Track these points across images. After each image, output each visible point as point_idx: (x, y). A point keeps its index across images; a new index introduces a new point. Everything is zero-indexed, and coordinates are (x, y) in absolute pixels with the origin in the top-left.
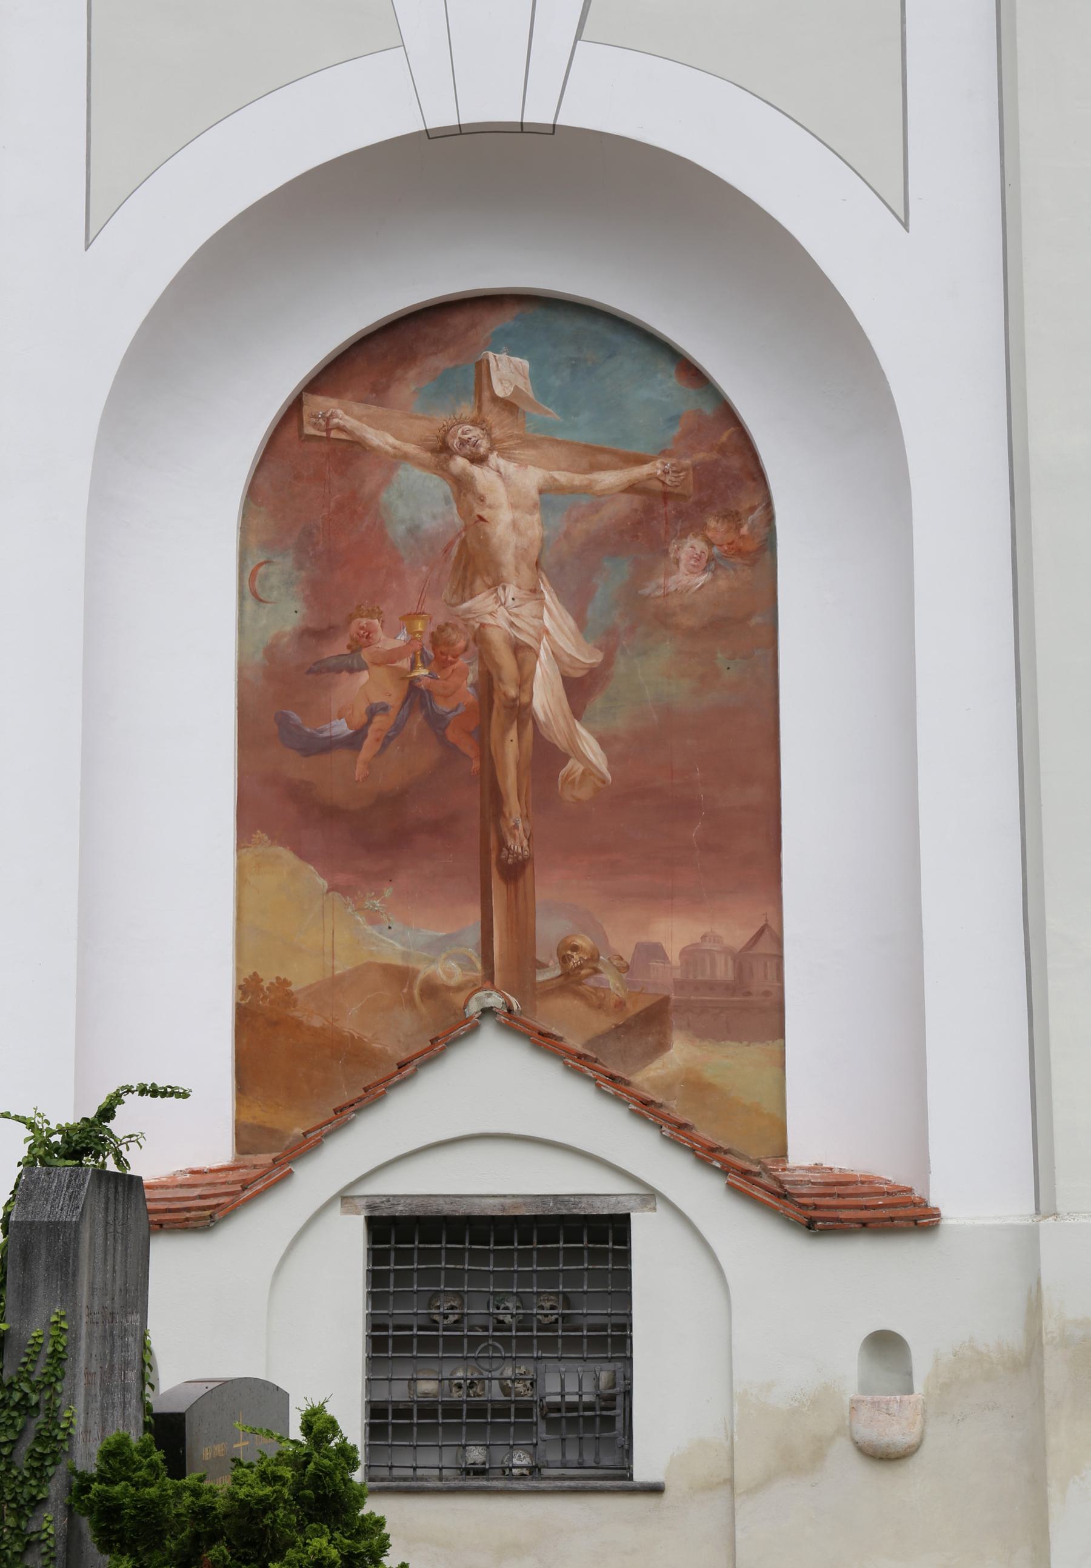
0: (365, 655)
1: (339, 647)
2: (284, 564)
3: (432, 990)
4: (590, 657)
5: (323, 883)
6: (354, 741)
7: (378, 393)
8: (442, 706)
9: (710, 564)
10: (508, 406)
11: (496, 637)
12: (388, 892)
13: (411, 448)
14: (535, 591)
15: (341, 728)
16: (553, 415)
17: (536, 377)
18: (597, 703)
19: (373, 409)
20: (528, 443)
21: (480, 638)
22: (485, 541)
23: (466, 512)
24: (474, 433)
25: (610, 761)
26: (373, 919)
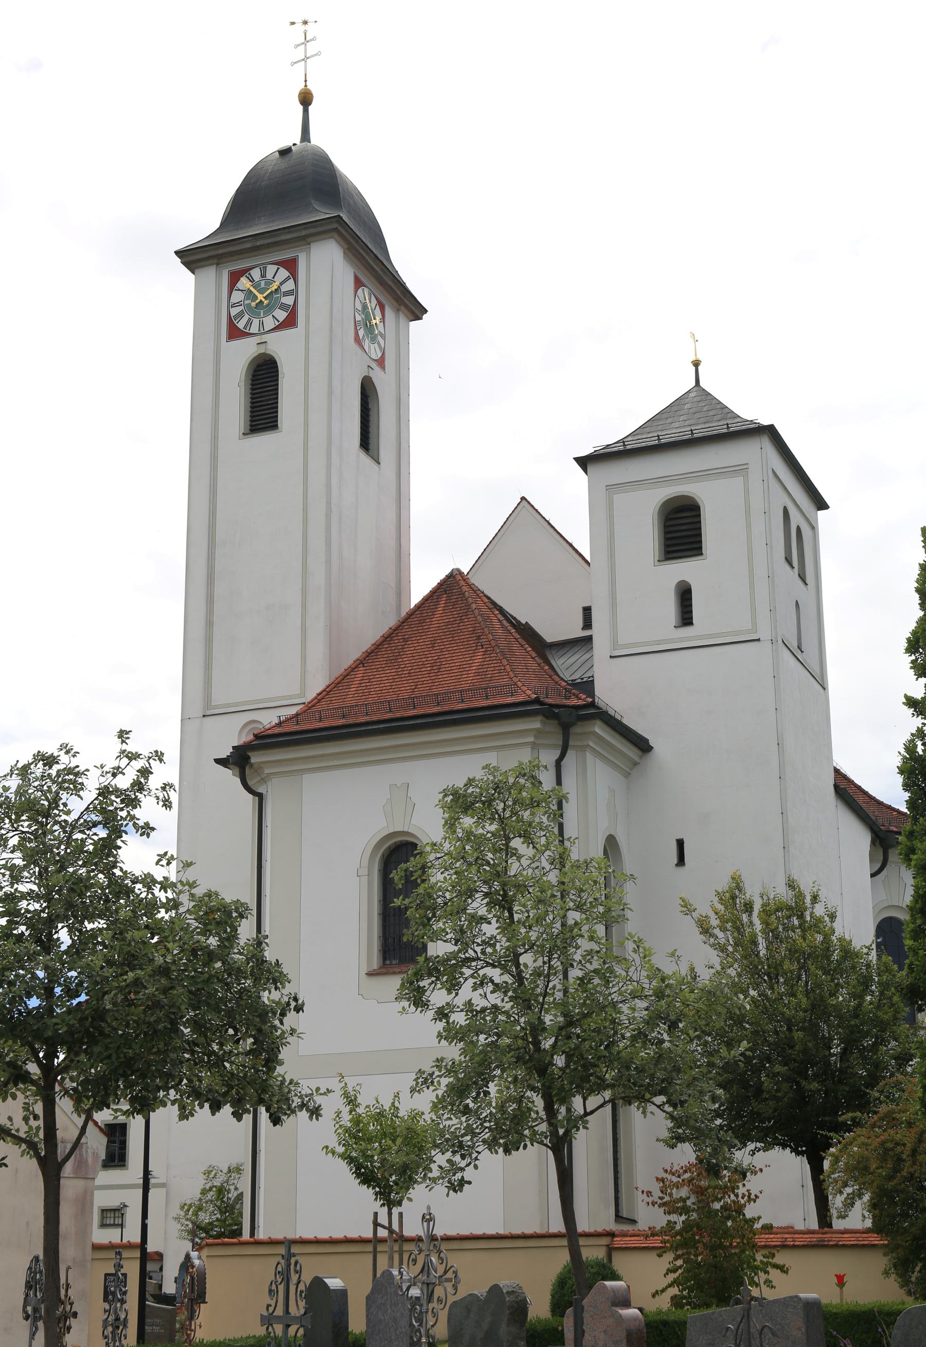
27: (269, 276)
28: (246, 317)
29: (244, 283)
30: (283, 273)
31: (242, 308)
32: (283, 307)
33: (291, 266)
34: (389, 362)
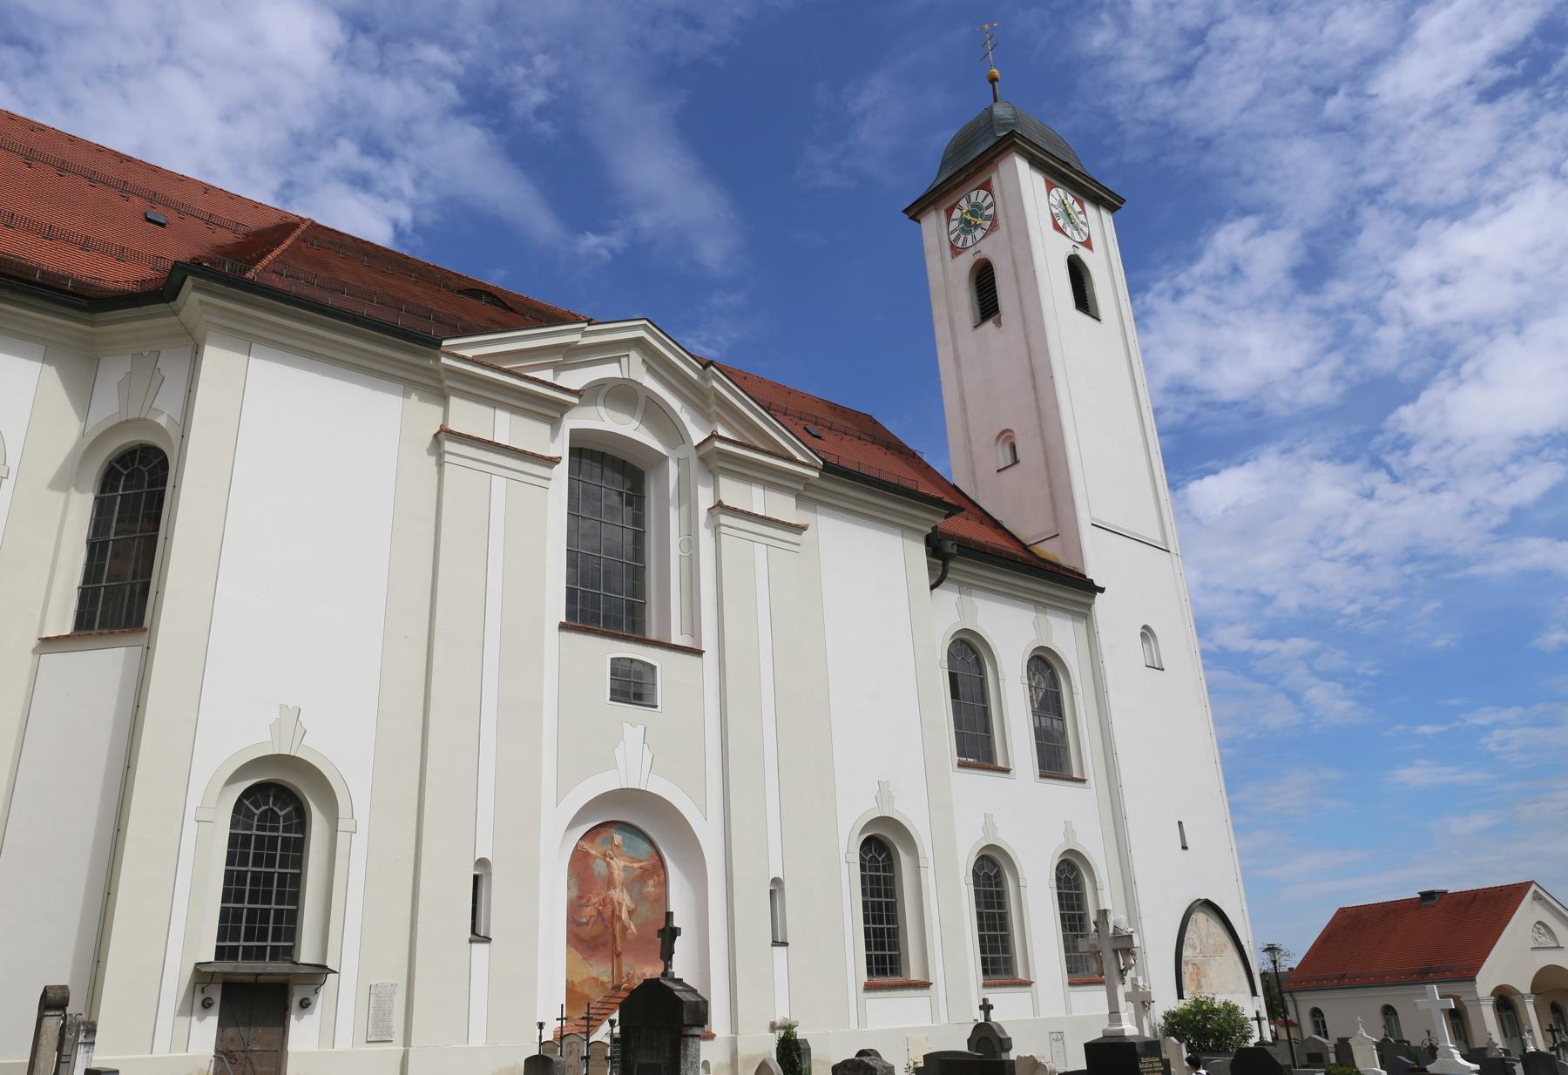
0: (590, 903)
1: (584, 901)
2: (574, 880)
3: (602, 983)
4: (633, 906)
5: (581, 957)
6: (587, 923)
7: (592, 841)
8: (605, 916)
9: (655, 886)
10: (617, 846)
11: (615, 901)
12: (594, 960)
13: (599, 855)
14: (622, 890)
15: (585, 920)
16: (625, 849)
17: (623, 840)
18: (634, 917)
19: (592, 845)
20: (621, 855)
21: (612, 900)
22: (613, 877)
23: (609, 871)
24: (611, 852)
25: (637, 930)
26: (591, 966)
27: (973, 200)
28: (962, 237)
29: (956, 214)
30: (983, 193)
31: (956, 233)
32: (987, 218)
33: (987, 186)
34: (1096, 242)
